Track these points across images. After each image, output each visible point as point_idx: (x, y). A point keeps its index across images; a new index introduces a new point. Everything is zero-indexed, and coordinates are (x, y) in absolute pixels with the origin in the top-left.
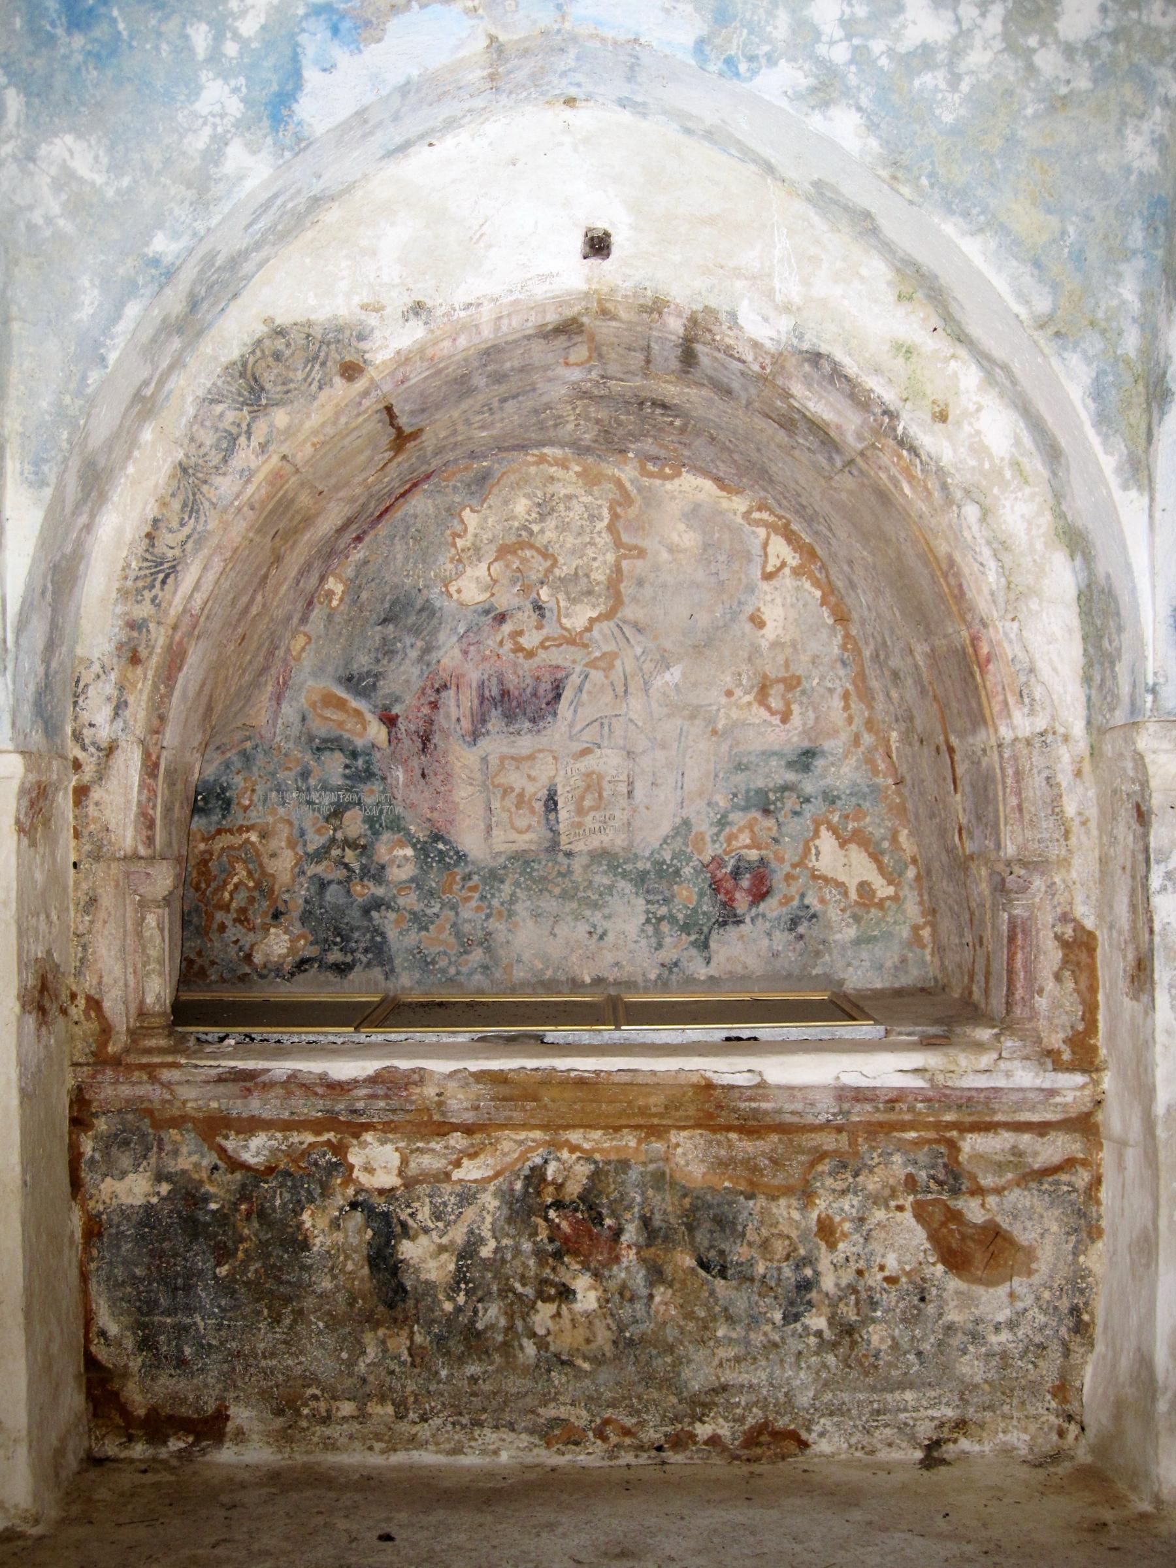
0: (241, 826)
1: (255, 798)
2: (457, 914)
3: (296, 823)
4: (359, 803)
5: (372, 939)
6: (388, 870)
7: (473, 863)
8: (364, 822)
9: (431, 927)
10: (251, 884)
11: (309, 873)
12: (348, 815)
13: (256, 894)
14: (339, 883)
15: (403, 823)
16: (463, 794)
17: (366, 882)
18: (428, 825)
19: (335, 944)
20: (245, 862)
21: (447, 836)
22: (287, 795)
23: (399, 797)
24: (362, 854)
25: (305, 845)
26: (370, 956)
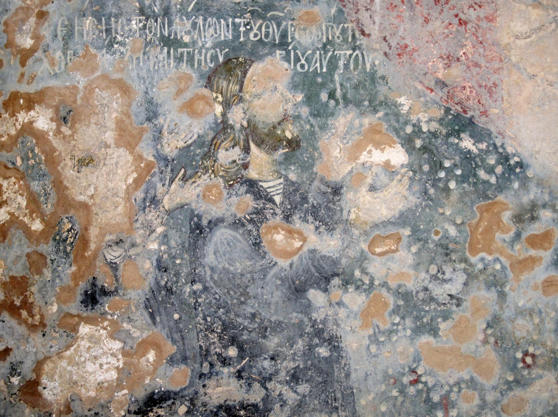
0: (15, 96)
1: (46, 32)
2: (502, 295)
3: (138, 88)
4: (283, 44)
5: (311, 348)
6: (348, 196)
7: (540, 183)
8: (294, 87)
9: (443, 326)
10: (37, 226)
11: (167, 203)
12: (256, 69)
13: (47, 248)
14: (237, 224)
15: (382, 89)
16: (519, 27)
17: (297, 224)
18: (439, 94)
19: (225, 361)
20: (22, 176)
21: (481, 121)
22: (118, 25)
23: (375, 31)
24: (287, 160)
25: (158, 137)
26: (304, 388)
